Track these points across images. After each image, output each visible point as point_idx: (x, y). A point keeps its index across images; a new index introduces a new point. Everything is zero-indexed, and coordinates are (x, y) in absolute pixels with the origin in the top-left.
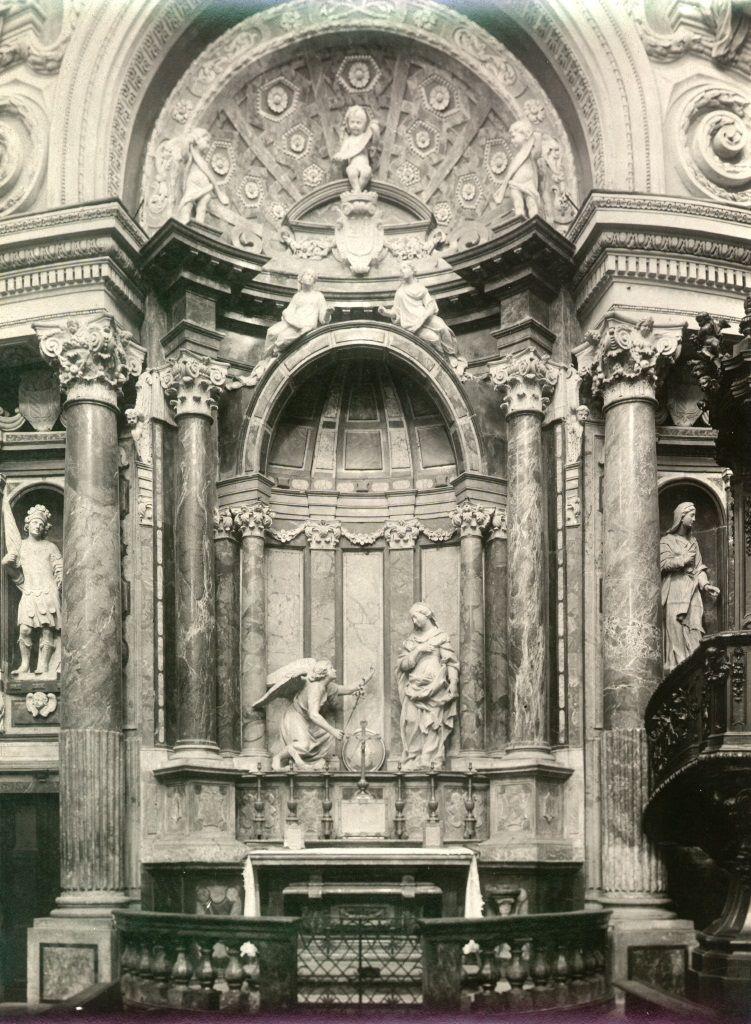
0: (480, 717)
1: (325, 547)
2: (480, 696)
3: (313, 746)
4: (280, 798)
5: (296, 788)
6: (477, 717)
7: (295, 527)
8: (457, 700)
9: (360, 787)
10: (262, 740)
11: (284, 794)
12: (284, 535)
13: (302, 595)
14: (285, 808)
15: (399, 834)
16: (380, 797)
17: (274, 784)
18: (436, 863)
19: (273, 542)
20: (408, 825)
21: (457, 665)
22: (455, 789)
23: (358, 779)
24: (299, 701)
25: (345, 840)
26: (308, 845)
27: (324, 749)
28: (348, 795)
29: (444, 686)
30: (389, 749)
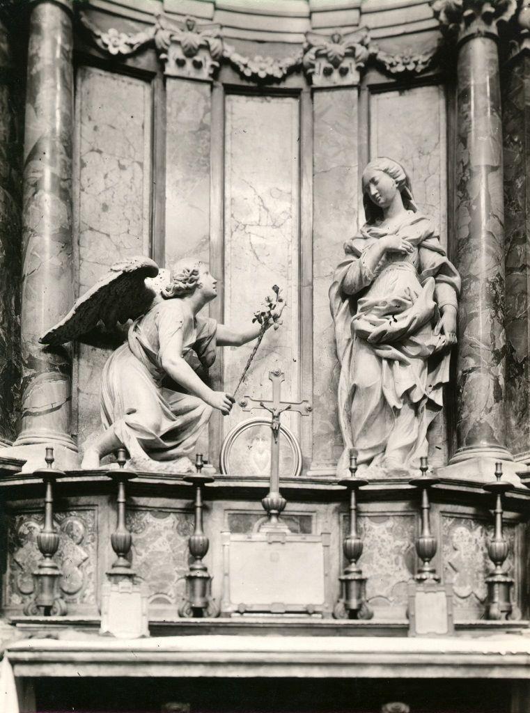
0: (502, 382)
1: (193, 74)
2: (500, 343)
3: (167, 426)
4: (96, 530)
5: (132, 509)
6: (497, 381)
7: (136, 32)
8: (454, 351)
9: (267, 508)
10: (62, 413)
11: (100, 523)
12: (115, 40)
13: (147, 163)
14: (109, 555)
15: (351, 609)
16: (306, 531)
17: (83, 500)
18: (472, 674)
19: (95, 53)
20: (369, 589)
21: (456, 279)
22: (459, 518)
23: (266, 491)
24: (139, 334)
25: (236, 619)
26: (157, 629)
27: (189, 439)
28: (240, 524)
29: (433, 318)
30: (308, 455)
